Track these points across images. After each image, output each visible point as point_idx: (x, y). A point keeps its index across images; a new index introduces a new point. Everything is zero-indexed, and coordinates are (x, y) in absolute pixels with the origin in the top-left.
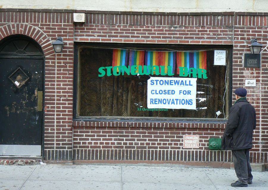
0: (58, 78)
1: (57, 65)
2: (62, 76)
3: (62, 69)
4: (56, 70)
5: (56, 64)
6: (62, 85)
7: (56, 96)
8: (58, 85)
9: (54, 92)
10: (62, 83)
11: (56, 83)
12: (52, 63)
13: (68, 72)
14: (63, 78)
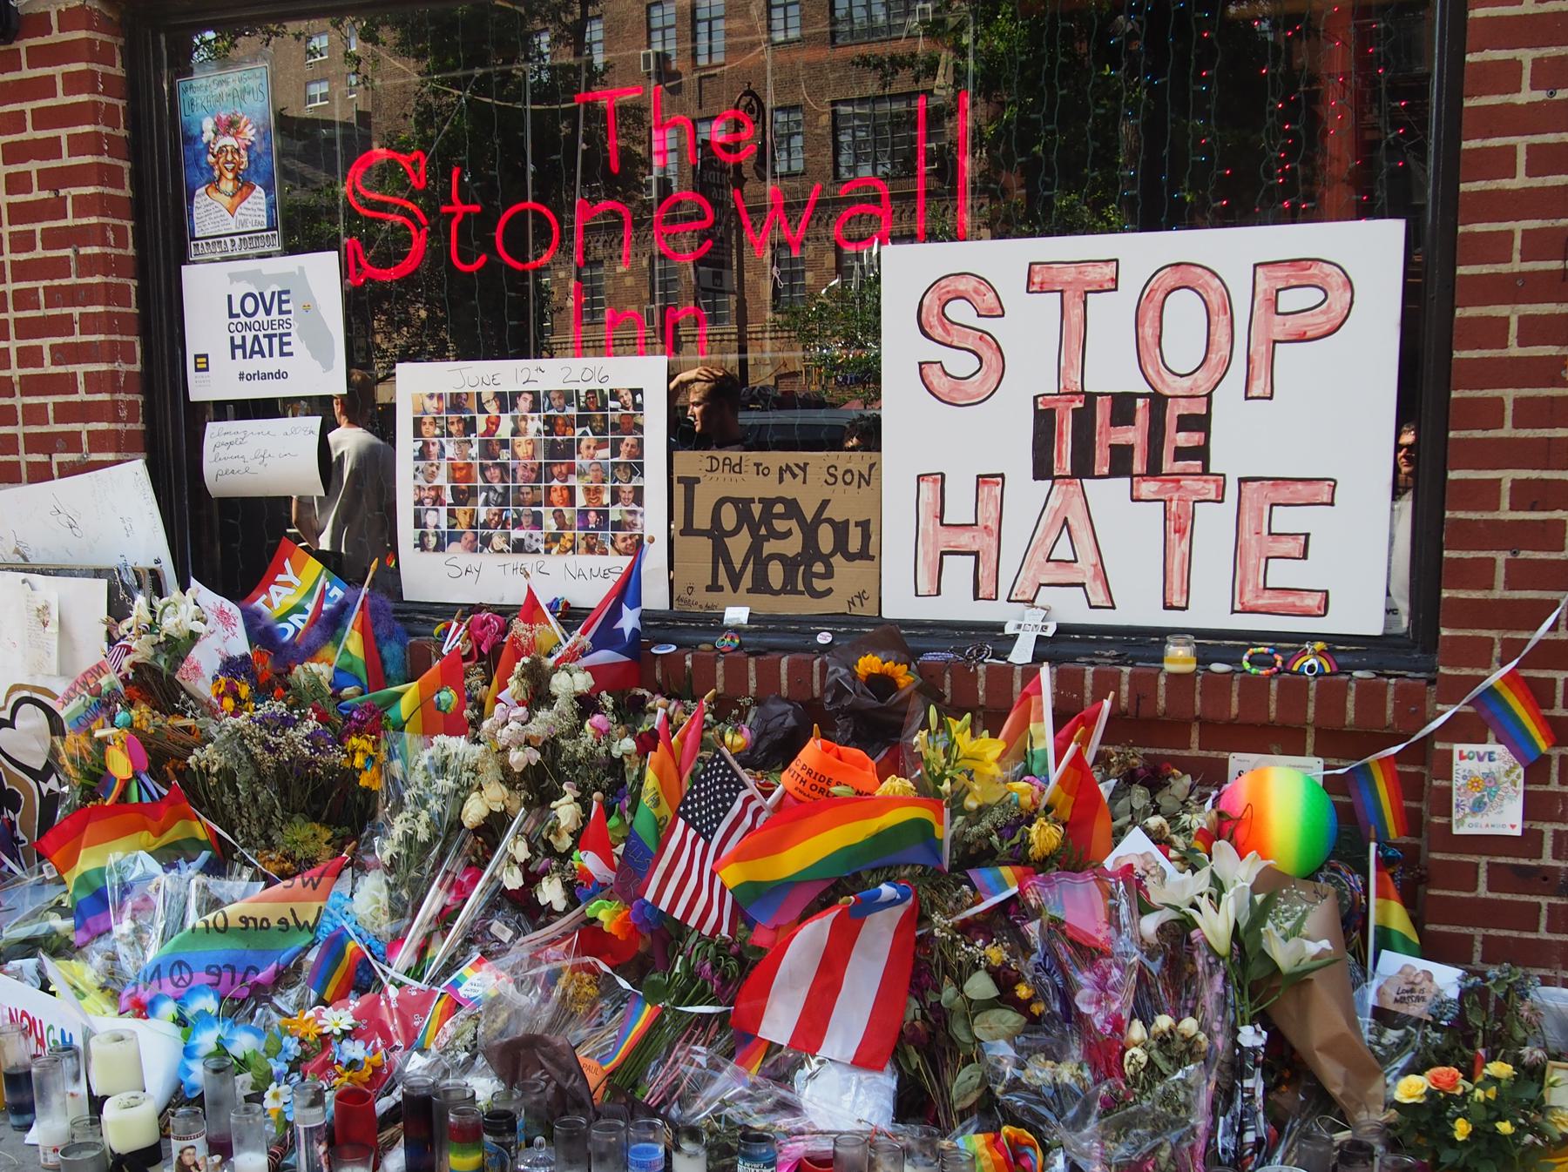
3: (38, 227)
10: (46, 343)
13: (77, 252)
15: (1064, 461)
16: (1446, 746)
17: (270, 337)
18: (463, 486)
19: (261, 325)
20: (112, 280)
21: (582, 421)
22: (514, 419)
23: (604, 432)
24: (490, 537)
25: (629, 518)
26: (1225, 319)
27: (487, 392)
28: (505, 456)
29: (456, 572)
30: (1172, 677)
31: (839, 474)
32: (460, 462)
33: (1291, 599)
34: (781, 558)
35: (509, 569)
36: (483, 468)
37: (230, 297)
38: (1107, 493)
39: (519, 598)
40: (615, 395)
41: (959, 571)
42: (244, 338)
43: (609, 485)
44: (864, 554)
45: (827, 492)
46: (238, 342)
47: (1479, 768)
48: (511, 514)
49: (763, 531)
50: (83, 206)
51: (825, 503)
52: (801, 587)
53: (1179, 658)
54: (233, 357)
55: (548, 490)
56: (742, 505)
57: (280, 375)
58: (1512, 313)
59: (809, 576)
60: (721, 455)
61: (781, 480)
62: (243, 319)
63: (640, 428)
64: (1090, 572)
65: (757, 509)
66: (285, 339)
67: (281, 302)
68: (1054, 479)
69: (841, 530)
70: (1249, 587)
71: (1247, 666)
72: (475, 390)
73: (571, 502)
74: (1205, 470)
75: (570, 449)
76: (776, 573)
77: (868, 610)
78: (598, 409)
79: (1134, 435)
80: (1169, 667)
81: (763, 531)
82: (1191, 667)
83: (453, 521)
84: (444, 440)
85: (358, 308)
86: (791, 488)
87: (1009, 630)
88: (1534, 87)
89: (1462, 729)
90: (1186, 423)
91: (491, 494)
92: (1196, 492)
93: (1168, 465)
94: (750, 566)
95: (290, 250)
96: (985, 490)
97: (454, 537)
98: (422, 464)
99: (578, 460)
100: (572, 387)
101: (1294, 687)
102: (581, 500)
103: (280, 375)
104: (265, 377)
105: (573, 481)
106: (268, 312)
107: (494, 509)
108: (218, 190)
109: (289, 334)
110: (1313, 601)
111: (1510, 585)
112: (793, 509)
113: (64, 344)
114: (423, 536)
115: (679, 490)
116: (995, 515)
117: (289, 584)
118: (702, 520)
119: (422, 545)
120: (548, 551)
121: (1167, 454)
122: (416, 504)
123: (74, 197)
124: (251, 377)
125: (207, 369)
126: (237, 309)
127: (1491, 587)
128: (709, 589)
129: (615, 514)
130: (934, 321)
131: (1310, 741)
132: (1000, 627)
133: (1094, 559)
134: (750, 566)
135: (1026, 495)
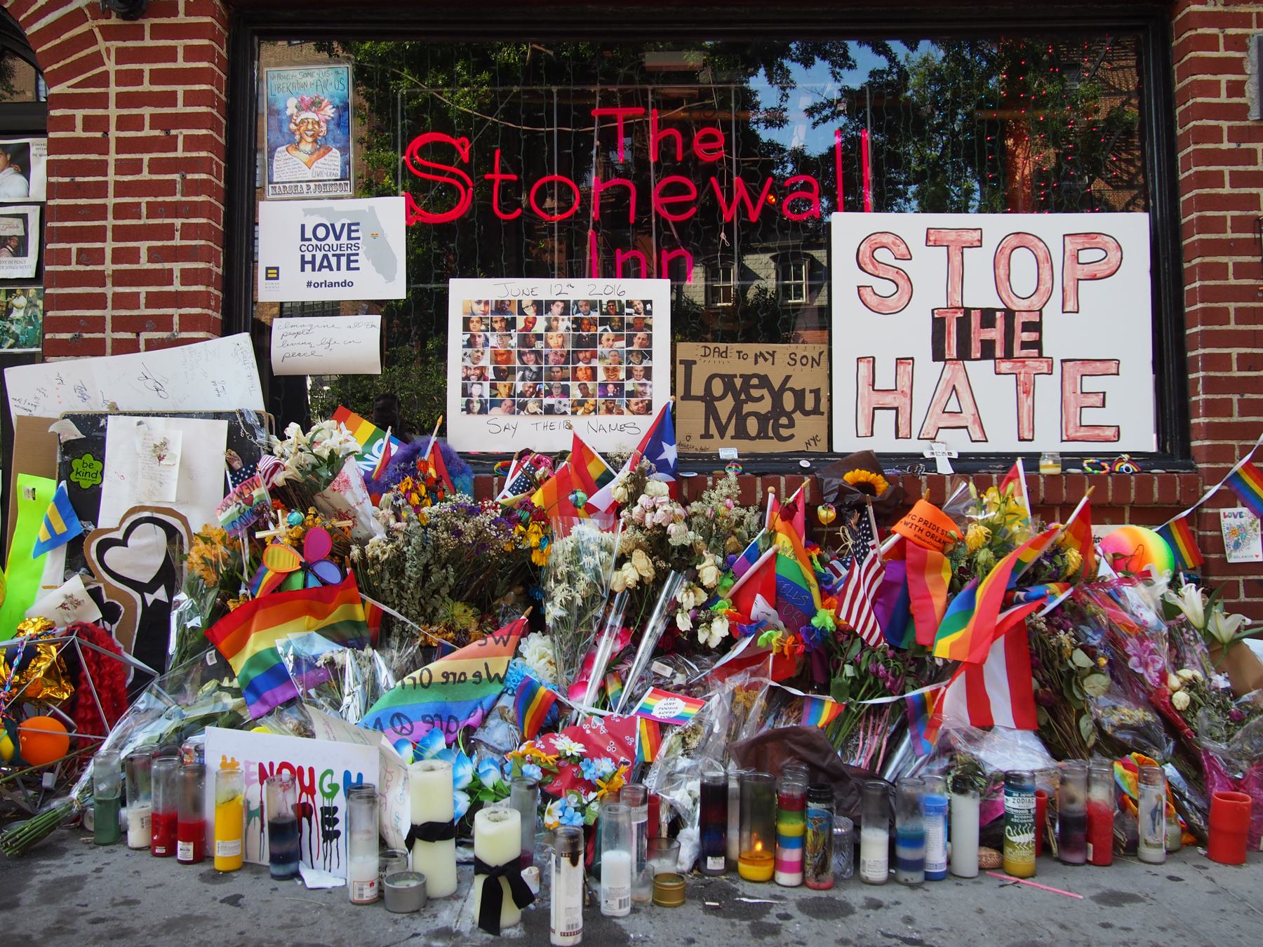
0: (120, 211)
1: (118, 139)
3: (146, 157)
4: (111, 169)
5: (113, 134)
7: (109, 326)
8: (118, 256)
9: (99, 301)
10: (144, 246)
11: (109, 246)
12: (89, 123)
13: (183, 178)
14: (154, 210)
15: (952, 350)
16: (1215, 511)
17: (338, 257)
18: (504, 366)
20: (212, 200)
21: (603, 322)
22: (548, 320)
23: (621, 329)
25: (641, 389)
27: (527, 301)
28: (539, 345)
30: (1051, 477)
32: (501, 350)
33: (1097, 432)
35: (540, 426)
36: (520, 354)
37: (303, 226)
38: (980, 369)
40: (630, 304)
41: (885, 420)
42: (314, 256)
43: (624, 366)
44: (816, 411)
45: (789, 371)
46: (308, 258)
47: (1234, 522)
48: (544, 386)
49: (743, 397)
50: (191, 143)
51: (788, 378)
52: (771, 434)
53: (1048, 467)
54: (303, 270)
55: (575, 370)
56: (728, 380)
57: (345, 284)
58: (1230, 260)
60: (712, 345)
61: (756, 362)
62: (314, 242)
63: (650, 327)
64: (971, 419)
65: (738, 382)
66: (352, 258)
67: (350, 231)
68: (946, 361)
69: (799, 395)
70: (1071, 425)
71: (1090, 470)
72: (517, 299)
73: (594, 377)
74: (1040, 355)
75: (594, 341)
76: (752, 425)
77: (822, 447)
79: (996, 334)
80: (1042, 471)
81: (743, 397)
82: (1057, 470)
83: (495, 392)
84: (488, 334)
85: (416, 234)
86: (763, 368)
87: (927, 455)
88: (1229, 141)
89: (1222, 500)
90: (1027, 327)
91: (527, 373)
92: (1035, 369)
93: (1017, 352)
94: (733, 421)
96: (901, 368)
97: (495, 403)
98: (469, 351)
99: (599, 349)
100: (597, 298)
101: (1121, 478)
102: (601, 377)
103: (345, 284)
104: (331, 285)
105: (595, 363)
106: (338, 238)
107: (530, 383)
108: (297, 149)
110: (1110, 433)
111: (1242, 414)
112: (764, 381)
113: (163, 247)
114: (468, 403)
115: (681, 369)
116: (908, 384)
118: (698, 389)
119: (468, 409)
121: (1017, 345)
123: (185, 136)
124: (317, 285)
125: (277, 278)
126: (309, 234)
127: (1231, 415)
128: (702, 437)
129: (629, 386)
130: (867, 261)
131: (1127, 515)
133: (973, 411)
134: (733, 421)
135: (928, 371)
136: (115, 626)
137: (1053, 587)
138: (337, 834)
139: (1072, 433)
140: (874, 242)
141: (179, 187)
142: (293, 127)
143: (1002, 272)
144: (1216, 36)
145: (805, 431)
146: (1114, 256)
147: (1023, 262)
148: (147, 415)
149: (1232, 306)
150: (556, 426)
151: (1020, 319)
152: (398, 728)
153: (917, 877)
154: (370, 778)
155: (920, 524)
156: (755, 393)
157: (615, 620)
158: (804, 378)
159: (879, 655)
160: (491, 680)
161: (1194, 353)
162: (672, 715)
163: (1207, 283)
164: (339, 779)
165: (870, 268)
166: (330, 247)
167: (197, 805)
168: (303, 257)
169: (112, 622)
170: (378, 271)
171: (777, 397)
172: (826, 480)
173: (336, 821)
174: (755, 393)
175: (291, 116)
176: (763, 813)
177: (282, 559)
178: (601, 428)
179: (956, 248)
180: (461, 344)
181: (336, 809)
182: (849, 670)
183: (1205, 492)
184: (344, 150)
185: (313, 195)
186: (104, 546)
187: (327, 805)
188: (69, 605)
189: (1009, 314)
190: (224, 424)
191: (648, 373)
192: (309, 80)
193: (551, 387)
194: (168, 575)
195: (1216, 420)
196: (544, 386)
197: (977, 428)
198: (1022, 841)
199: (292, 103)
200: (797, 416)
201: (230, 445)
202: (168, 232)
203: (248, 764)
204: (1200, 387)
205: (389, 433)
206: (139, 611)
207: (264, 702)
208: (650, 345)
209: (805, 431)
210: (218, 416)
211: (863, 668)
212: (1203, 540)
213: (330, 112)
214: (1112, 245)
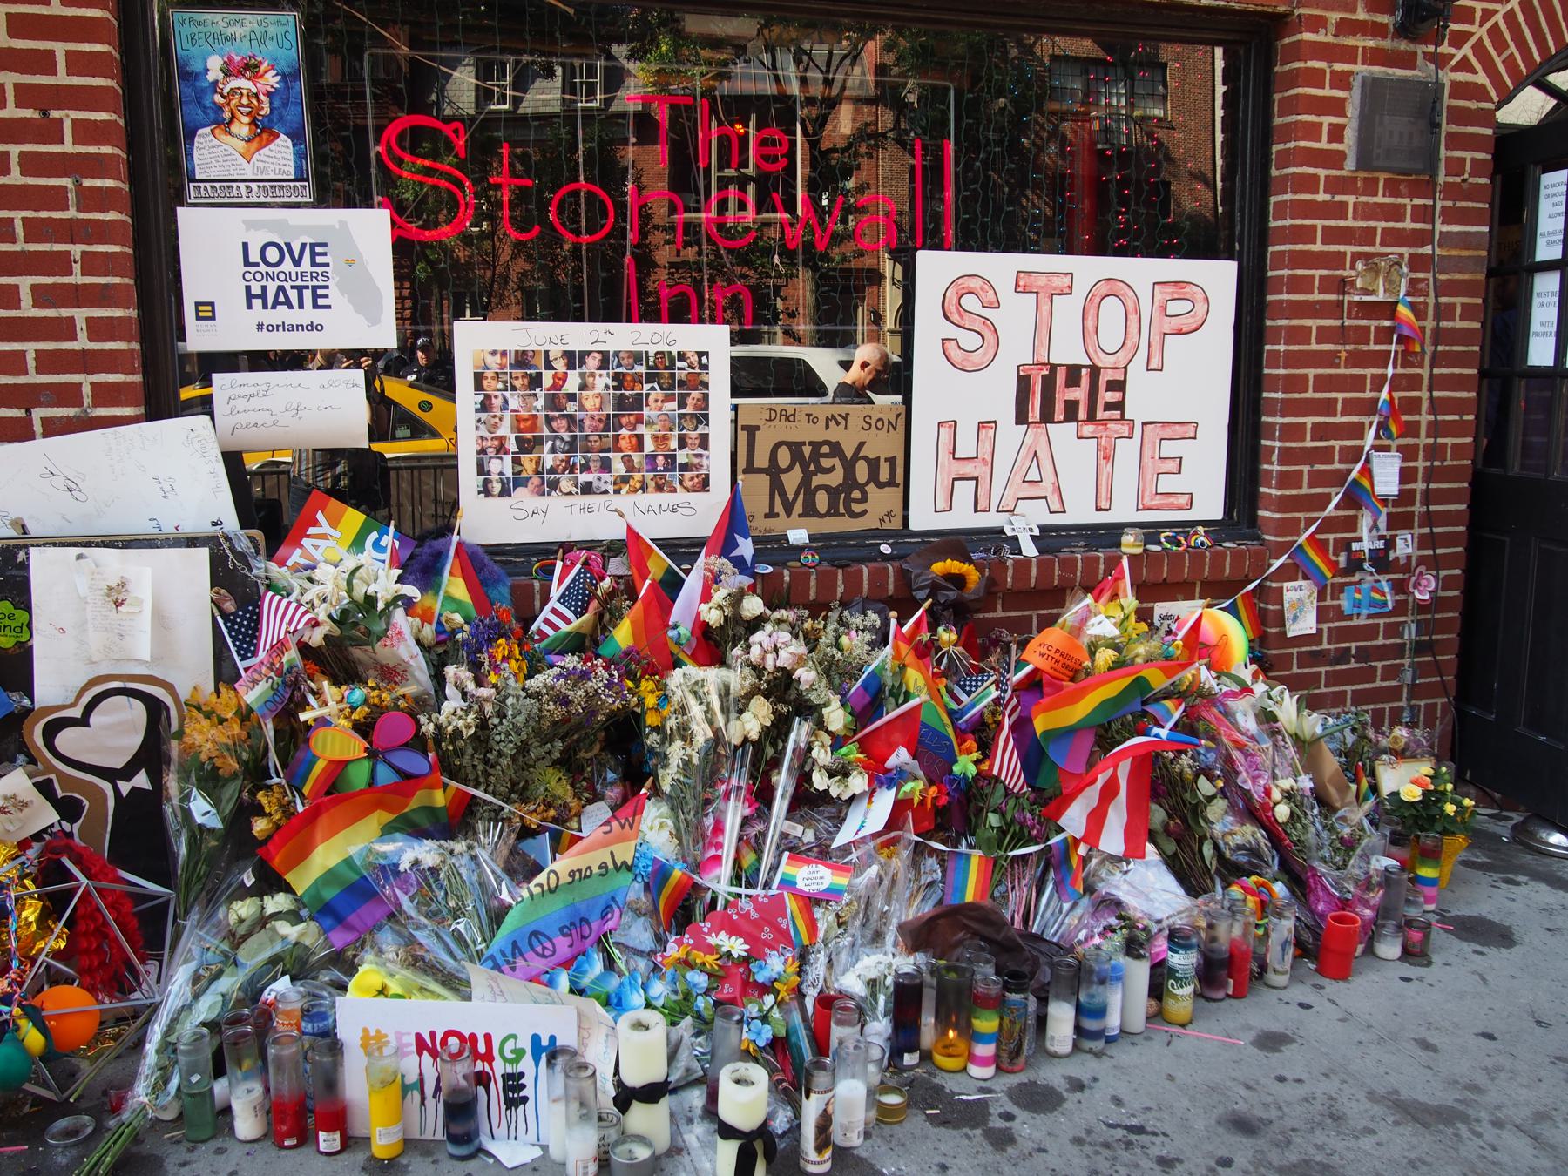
2: (18, 215)
6: (26, 298)
10: (25, 283)
13: (78, 184)
15: (1035, 413)
17: (300, 289)
18: (528, 435)
19: (288, 276)
21: (650, 378)
22: (582, 375)
23: (671, 387)
24: (557, 482)
25: (696, 461)
26: (1135, 318)
28: (572, 408)
29: (523, 514)
31: (873, 422)
32: (525, 414)
33: (1171, 500)
34: (826, 488)
36: (549, 420)
37: (245, 246)
38: (1062, 433)
39: (620, 534)
40: (682, 356)
41: (965, 490)
42: (264, 288)
43: (676, 432)
44: (891, 483)
45: (863, 436)
46: (256, 290)
48: (579, 459)
49: (812, 468)
51: (862, 444)
52: (842, 510)
54: (249, 306)
55: (617, 438)
56: (795, 448)
57: (311, 327)
59: (848, 501)
61: (827, 427)
62: (263, 268)
63: (706, 385)
65: (807, 450)
66: (320, 292)
67: (313, 255)
68: (1028, 424)
69: (874, 465)
70: (1147, 494)
72: (543, 349)
73: (639, 446)
74: (1122, 418)
75: (638, 402)
76: (822, 501)
77: (896, 524)
78: (666, 368)
79: (1080, 394)
80: (1124, 549)
81: (812, 468)
82: (1139, 550)
83: (518, 468)
84: (507, 394)
86: (835, 433)
87: (1009, 533)
89: (1287, 573)
91: (558, 443)
93: (1100, 414)
94: (801, 496)
95: (325, 198)
96: (983, 432)
97: (519, 483)
98: (484, 416)
99: (646, 412)
100: (643, 348)
101: (1197, 555)
102: (649, 446)
103: (311, 327)
104: (292, 328)
105: (641, 429)
106: (297, 263)
107: (562, 456)
109: (326, 287)
110: (1183, 500)
112: (836, 450)
113: (54, 285)
114: (486, 483)
115: (743, 436)
117: (324, 537)
118: (762, 460)
119: (486, 491)
120: (617, 492)
121: (1100, 406)
122: (479, 453)
123: (74, 122)
124: (272, 328)
125: (213, 318)
126: (254, 256)
128: (767, 516)
129: (682, 457)
130: (953, 308)
132: (1001, 531)
133: (1053, 479)
134: (801, 496)
135: (1010, 434)
136: (77, 826)
137: (1168, 703)
138: (525, 1100)
139: (1148, 502)
140: (960, 287)
141: (72, 197)
142: (218, 99)
143: (1090, 324)
144: (1323, 71)
145: (878, 506)
146: (1201, 308)
147: (1112, 311)
148: (88, 545)
149: (1311, 372)
150: (595, 508)
151: (1105, 377)
152: (539, 949)
153: (1098, 1045)
154: (566, 1039)
155: (1057, 656)
156: (826, 463)
157: (738, 779)
158: (882, 445)
159: (1025, 803)
160: (617, 869)
161: (1270, 419)
162: (822, 888)
163: (1292, 348)
164: (525, 1043)
165: (955, 317)
166: (288, 277)
167: (331, 1083)
168: (248, 288)
169: (72, 821)
170: (358, 310)
171: (849, 467)
172: (915, 571)
173: (523, 1087)
174: (826, 463)
175: (216, 82)
176: (958, 1005)
177: (336, 744)
178: (650, 510)
179: (1046, 294)
180: (473, 407)
181: (522, 1075)
182: (994, 819)
183: (1270, 565)
184: (296, 137)
185: (256, 200)
186: (52, 730)
187: (509, 1070)
188: (11, 809)
189: (1095, 371)
190: (204, 553)
191: (704, 441)
192: (238, 30)
193: (587, 460)
194: (151, 755)
195: (1288, 492)
196: (579, 459)
197: (1056, 499)
198: (1182, 995)
199: (215, 64)
200: (871, 488)
201: (215, 581)
202: (62, 264)
203: (399, 1035)
204: (1275, 457)
205: (392, 529)
206: (111, 804)
207: (350, 928)
208: (707, 408)
209: (878, 506)
210: (192, 542)
211: (1009, 817)
212: (1264, 612)
213: (272, 80)
214: (1199, 296)
